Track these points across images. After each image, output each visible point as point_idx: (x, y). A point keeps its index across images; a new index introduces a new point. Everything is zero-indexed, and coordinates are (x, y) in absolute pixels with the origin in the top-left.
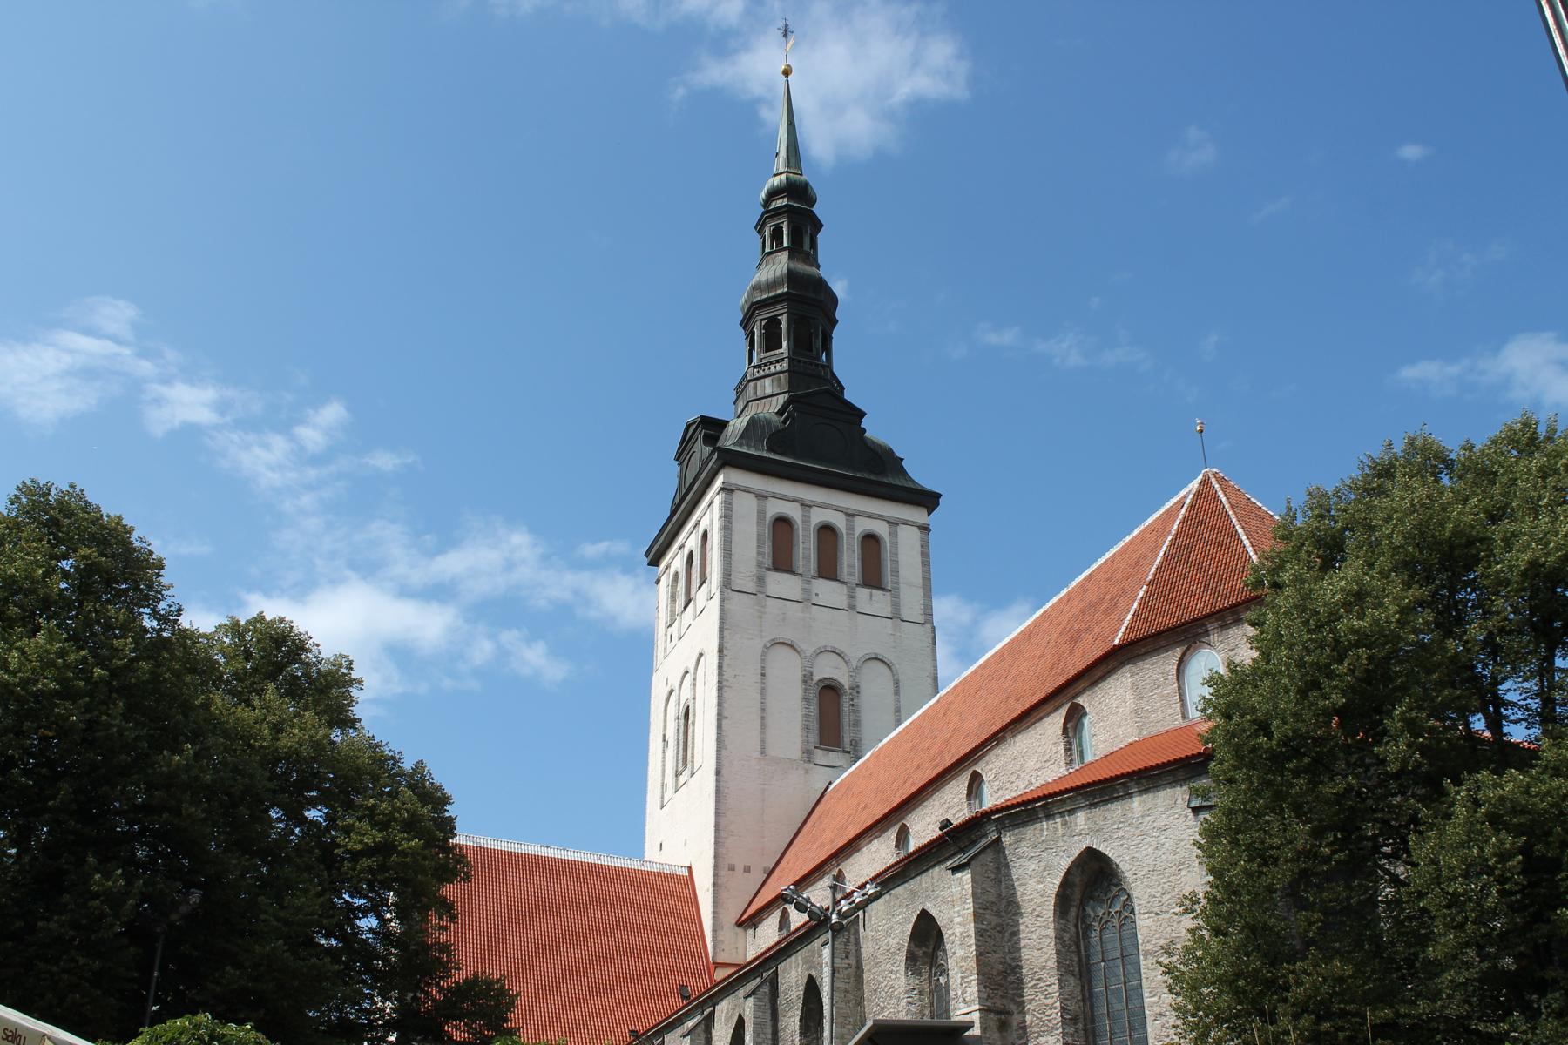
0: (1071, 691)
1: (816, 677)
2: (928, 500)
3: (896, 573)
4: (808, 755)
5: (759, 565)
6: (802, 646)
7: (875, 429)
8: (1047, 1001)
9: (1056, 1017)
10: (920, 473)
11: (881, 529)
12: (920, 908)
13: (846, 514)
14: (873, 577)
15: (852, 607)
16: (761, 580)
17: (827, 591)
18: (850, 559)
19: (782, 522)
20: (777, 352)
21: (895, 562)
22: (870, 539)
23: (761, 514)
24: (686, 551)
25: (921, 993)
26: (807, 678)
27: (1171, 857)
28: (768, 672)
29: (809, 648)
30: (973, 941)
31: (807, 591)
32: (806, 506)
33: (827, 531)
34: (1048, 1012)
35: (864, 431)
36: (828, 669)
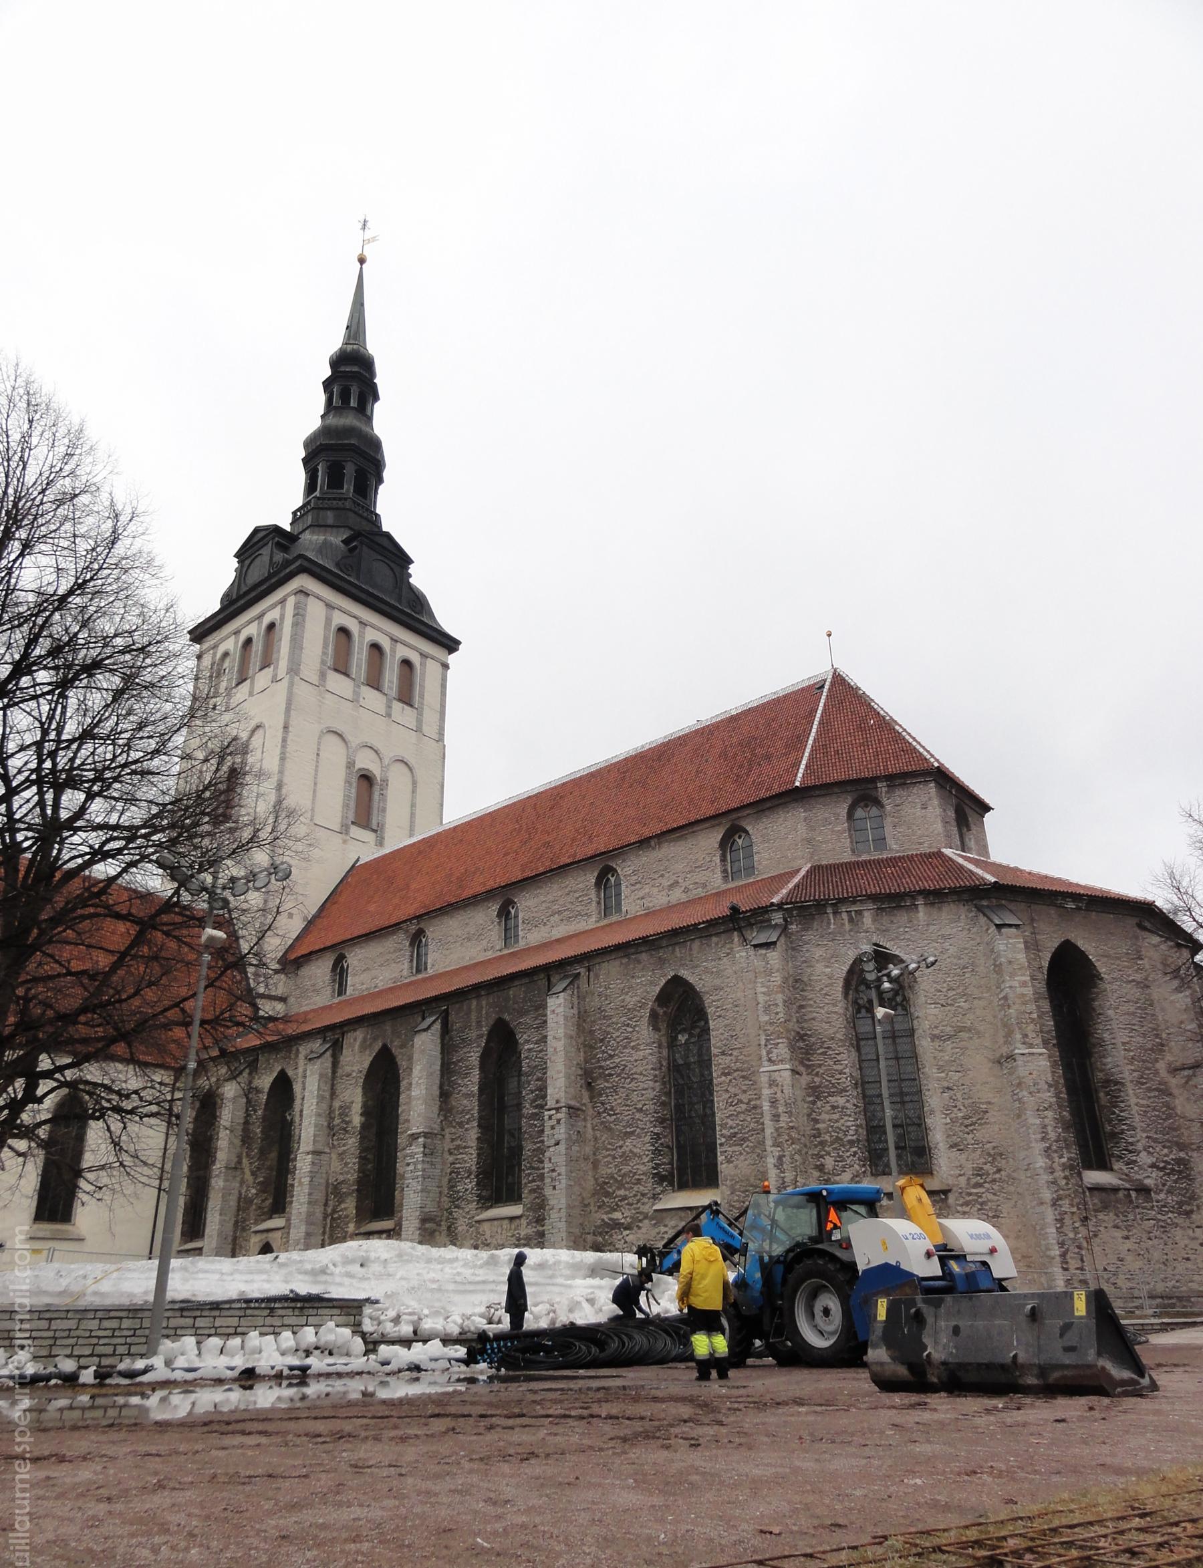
0: (735, 816)
1: (358, 765)
2: (451, 645)
3: (422, 696)
4: (344, 831)
5: (323, 662)
6: (349, 737)
7: (418, 577)
8: (835, 1067)
9: (845, 1081)
10: (446, 619)
11: (415, 658)
12: (672, 974)
13: (392, 639)
14: (406, 696)
15: (389, 715)
16: (323, 676)
17: (370, 697)
18: (391, 675)
19: (343, 631)
21: (422, 687)
22: (406, 663)
23: (328, 621)
24: (243, 637)
25: (660, 1046)
26: (350, 764)
27: (955, 961)
28: (321, 753)
29: (354, 741)
30: (780, 1009)
31: (357, 694)
32: (363, 624)
33: (376, 647)
34: (838, 1076)
35: (410, 576)
36: (365, 761)
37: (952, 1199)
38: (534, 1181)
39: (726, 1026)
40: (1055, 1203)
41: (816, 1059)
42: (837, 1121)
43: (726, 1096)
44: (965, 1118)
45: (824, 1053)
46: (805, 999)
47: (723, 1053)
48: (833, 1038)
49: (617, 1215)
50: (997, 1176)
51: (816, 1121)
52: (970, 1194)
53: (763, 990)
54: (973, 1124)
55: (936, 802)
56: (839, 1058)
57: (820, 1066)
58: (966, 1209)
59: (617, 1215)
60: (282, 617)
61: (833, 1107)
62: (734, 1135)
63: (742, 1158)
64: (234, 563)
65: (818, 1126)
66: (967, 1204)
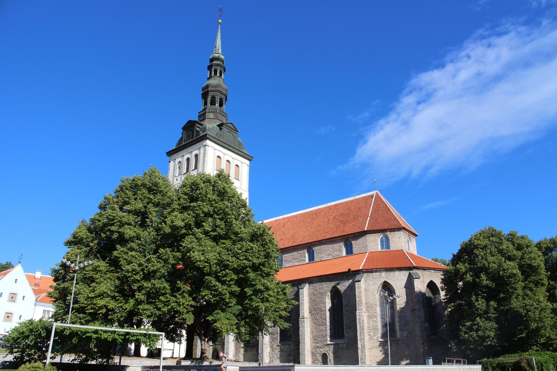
5: (213, 168)
11: (239, 164)
20: (214, 106)
23: (214, 154)
37: (400, 342)
38: (295, 335)
39: (347, 300)
40: (423, 343)
41: (370, 309)
42: (374, 324)
43: (347, 317)
44: (404, 324)
45: (371, 308)
46: (368, 294)
47: (346, 306)
48: (374, 304)
49: (318, 345)
50: (411, 337)
51: (369, 324)
52: (404, 341)
53: (358, 292)
54: (406, 325)
55: (403, 237)
56: (375, 309)
57: (370, 311)
58: (403, 345)
59: (318, 345)
60: (200, 154)
61: (373, 321)
62: (348, 327)
63: (351, 332)
64: (181, 131)
65: (370, 325)
66: (403, 343)
